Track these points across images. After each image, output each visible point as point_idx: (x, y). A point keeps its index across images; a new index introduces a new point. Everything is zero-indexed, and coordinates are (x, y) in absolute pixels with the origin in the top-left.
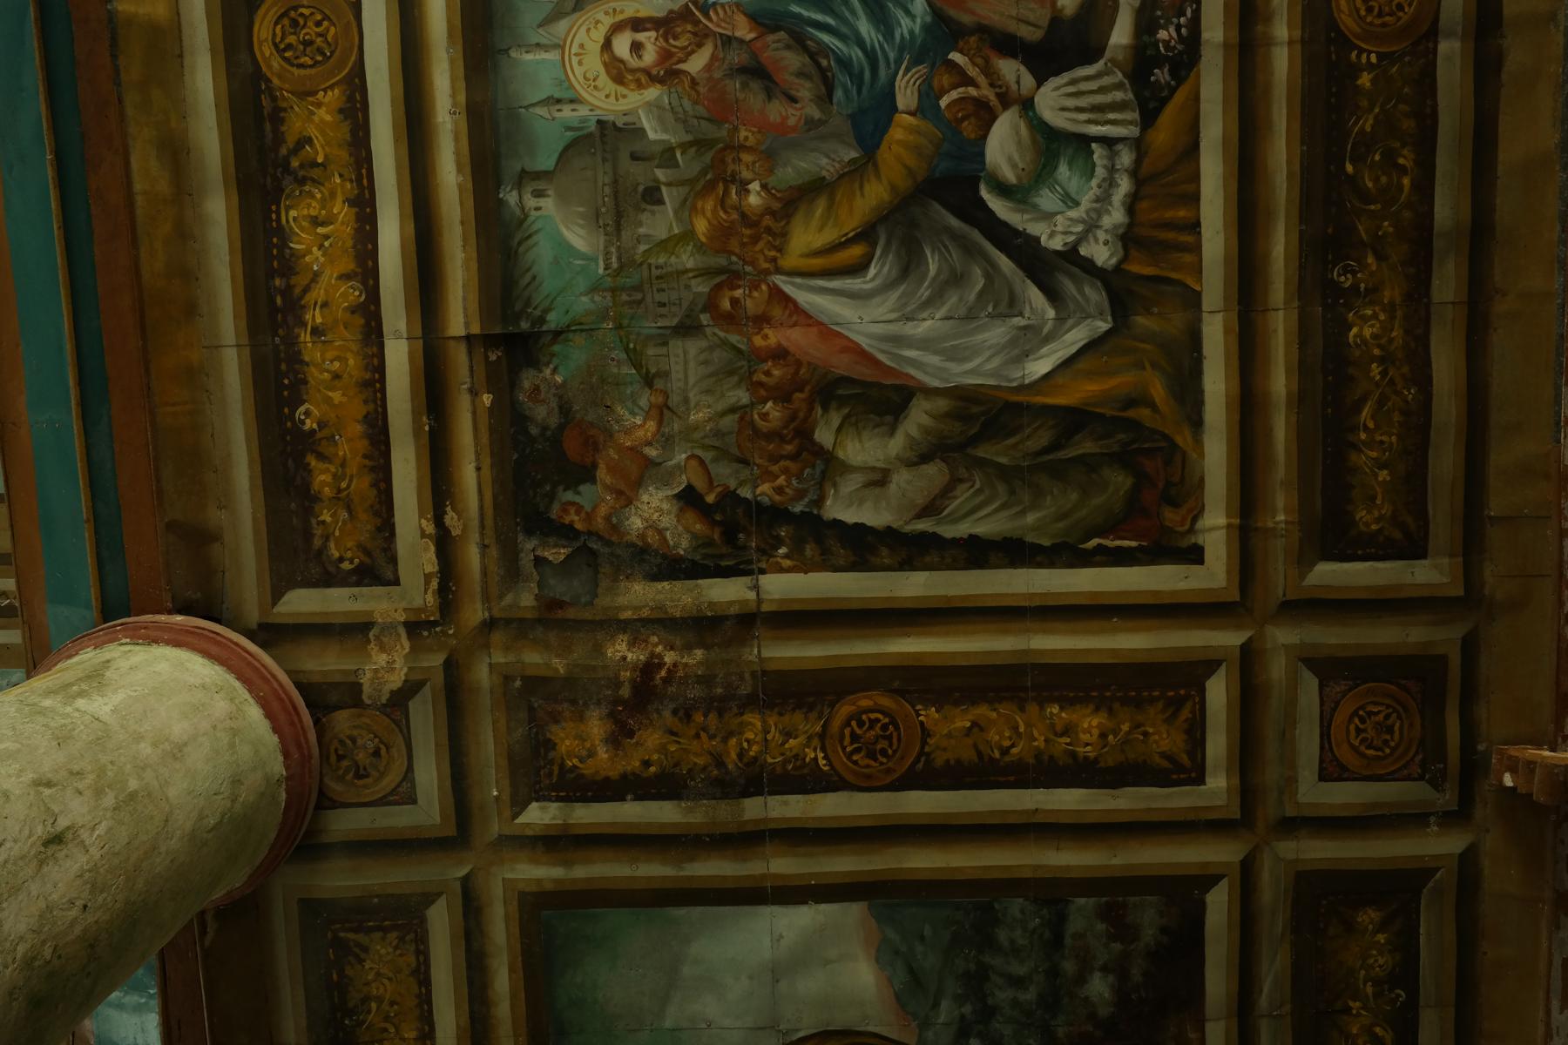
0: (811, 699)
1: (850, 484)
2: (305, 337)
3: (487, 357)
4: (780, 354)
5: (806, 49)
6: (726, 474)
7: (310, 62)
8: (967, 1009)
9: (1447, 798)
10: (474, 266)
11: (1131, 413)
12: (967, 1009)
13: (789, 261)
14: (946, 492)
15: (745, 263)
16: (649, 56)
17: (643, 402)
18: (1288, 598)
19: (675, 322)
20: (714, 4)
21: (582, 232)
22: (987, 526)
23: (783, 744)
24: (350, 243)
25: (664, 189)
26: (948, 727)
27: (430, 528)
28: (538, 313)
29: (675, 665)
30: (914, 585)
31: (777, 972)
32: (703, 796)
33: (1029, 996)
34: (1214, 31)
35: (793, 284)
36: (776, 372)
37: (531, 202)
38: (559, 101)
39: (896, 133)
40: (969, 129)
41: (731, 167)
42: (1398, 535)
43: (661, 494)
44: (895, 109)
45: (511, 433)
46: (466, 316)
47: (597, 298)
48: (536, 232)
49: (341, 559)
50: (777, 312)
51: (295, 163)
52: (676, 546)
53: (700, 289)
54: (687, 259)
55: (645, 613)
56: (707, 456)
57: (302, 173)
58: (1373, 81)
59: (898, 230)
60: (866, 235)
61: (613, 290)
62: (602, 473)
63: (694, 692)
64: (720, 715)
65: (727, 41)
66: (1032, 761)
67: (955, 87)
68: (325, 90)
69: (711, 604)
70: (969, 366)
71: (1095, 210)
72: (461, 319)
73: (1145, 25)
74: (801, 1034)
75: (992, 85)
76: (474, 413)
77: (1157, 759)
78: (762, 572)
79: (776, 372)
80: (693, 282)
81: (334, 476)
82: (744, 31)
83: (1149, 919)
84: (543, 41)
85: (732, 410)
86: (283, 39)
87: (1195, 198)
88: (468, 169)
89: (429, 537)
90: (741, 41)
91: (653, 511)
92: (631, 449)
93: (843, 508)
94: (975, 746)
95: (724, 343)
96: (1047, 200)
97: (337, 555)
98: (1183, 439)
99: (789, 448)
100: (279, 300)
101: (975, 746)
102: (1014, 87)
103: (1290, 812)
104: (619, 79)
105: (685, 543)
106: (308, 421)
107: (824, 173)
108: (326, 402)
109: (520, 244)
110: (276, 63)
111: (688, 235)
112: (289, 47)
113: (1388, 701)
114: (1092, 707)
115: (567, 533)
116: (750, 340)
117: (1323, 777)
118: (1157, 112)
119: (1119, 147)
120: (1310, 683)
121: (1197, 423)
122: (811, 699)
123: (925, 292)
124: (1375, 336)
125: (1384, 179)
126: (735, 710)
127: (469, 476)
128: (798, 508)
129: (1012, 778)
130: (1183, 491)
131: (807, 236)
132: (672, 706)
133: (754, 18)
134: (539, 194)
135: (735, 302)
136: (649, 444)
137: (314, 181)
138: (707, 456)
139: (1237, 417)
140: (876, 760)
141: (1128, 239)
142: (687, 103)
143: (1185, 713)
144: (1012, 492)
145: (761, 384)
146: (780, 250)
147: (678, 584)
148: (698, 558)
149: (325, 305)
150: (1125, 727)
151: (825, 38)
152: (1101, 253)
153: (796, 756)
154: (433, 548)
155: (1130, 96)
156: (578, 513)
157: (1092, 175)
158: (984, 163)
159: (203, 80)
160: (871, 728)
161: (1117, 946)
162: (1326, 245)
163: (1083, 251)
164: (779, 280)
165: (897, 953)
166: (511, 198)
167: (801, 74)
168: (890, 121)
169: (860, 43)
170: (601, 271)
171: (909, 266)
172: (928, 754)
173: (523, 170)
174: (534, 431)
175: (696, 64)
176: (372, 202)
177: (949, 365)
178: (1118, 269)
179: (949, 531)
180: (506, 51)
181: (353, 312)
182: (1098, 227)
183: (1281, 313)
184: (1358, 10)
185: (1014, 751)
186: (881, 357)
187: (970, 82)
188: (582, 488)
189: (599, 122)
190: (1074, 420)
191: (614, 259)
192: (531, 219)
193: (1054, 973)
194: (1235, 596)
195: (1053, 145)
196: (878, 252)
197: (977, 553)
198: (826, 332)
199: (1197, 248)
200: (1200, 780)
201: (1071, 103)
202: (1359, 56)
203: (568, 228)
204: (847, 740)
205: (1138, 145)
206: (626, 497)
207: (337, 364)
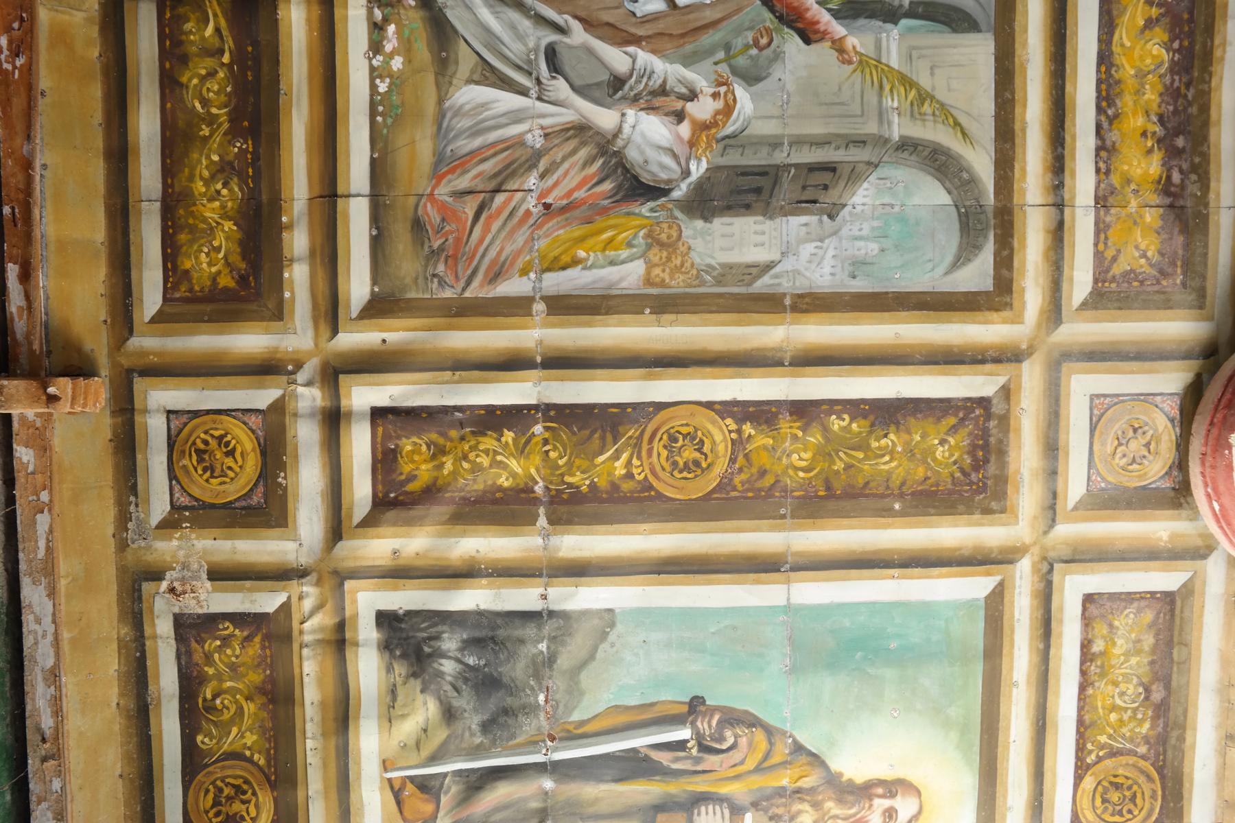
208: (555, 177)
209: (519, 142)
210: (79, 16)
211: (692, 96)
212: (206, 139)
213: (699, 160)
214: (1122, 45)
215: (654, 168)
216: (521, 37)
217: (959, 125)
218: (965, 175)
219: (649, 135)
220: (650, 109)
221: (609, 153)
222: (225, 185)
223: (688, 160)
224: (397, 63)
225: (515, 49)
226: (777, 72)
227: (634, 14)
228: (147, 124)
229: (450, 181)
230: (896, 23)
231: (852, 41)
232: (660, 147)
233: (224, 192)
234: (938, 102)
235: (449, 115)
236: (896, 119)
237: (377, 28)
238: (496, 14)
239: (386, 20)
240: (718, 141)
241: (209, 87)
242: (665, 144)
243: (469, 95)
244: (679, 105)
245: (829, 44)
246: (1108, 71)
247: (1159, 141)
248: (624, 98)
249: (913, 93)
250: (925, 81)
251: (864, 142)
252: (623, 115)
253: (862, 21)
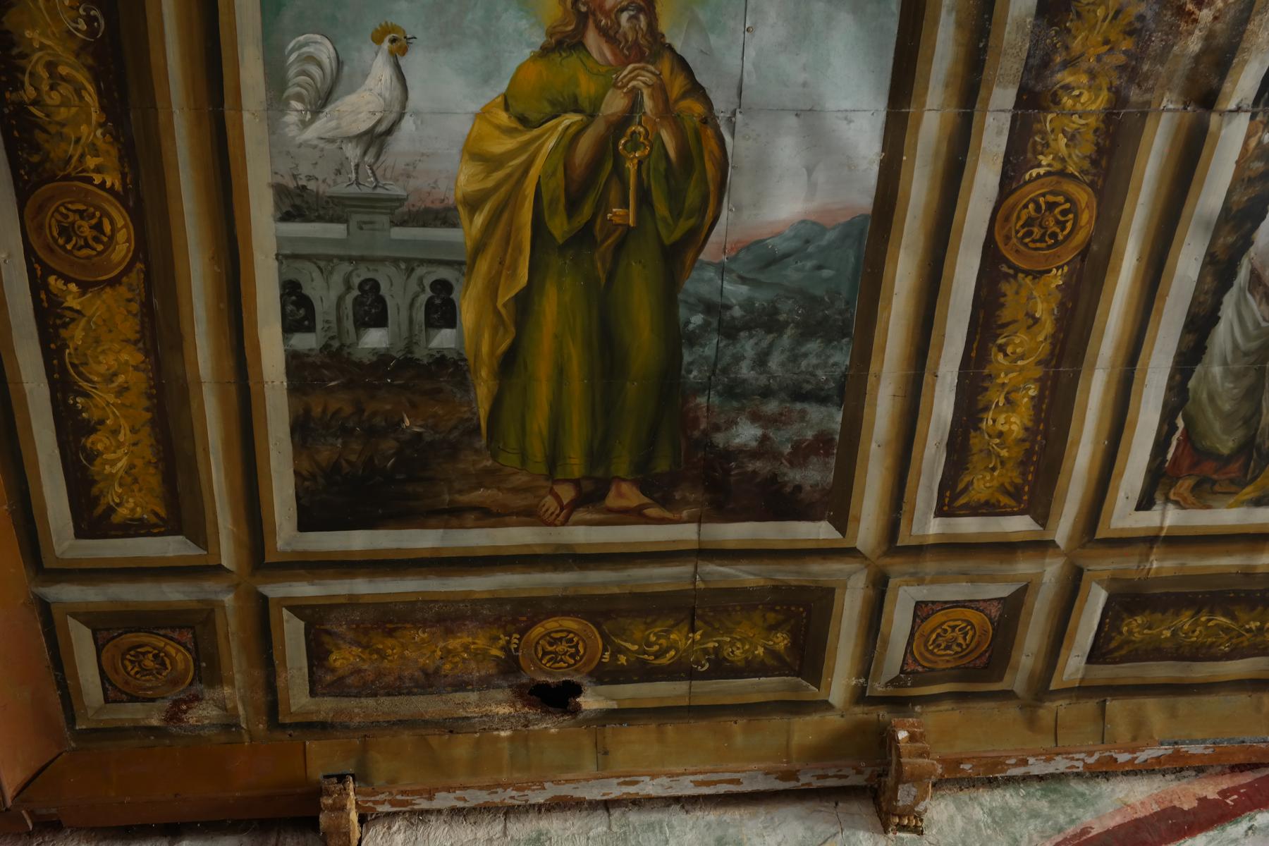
0: (1104, 163)
8: (737, 312)
9: (878, 688)
12: (737, 312)
18: (1086, 575)
22: (1223, 336)
23: (1064, 132)
26: (1040, 299)
29: (1196, 21)
31: (810, 115)
32: (1035, 44)
33: (745, 371)
42: (1113, 645)
63: (1156, 44)
64: (1118, 67)
66: (986, 371)
69: (1245, 62)
74: (728, 138)
77: (967, 479)
83: (814, 475)
94: (1014, 321)
98: (1249, 492)
101: (1014, 321)
103: (892, 582)
113: (973, 645)
114: (1030, 424)
117: (919, 604)
120: (1003, 591)
122: (1104, 163)
126: (1116, 82)
129: (973, 354)
130: (1203, 494)
132: (1149, 15)
139: (1252, 531)
140: (1023, 226)
143: (1005, 500)
144: (1246, 354)
150: (1004, 453)
153: (1047, 145)
160: (1058, 222)
161: (787, 449)
165: (807, 242)
172: (1015, 277)
179: (1229, 300)
185: (1000, 357)
193: (766, 393)
197: (1200, 323)
200: (940, 513)
204: (1051, 198)
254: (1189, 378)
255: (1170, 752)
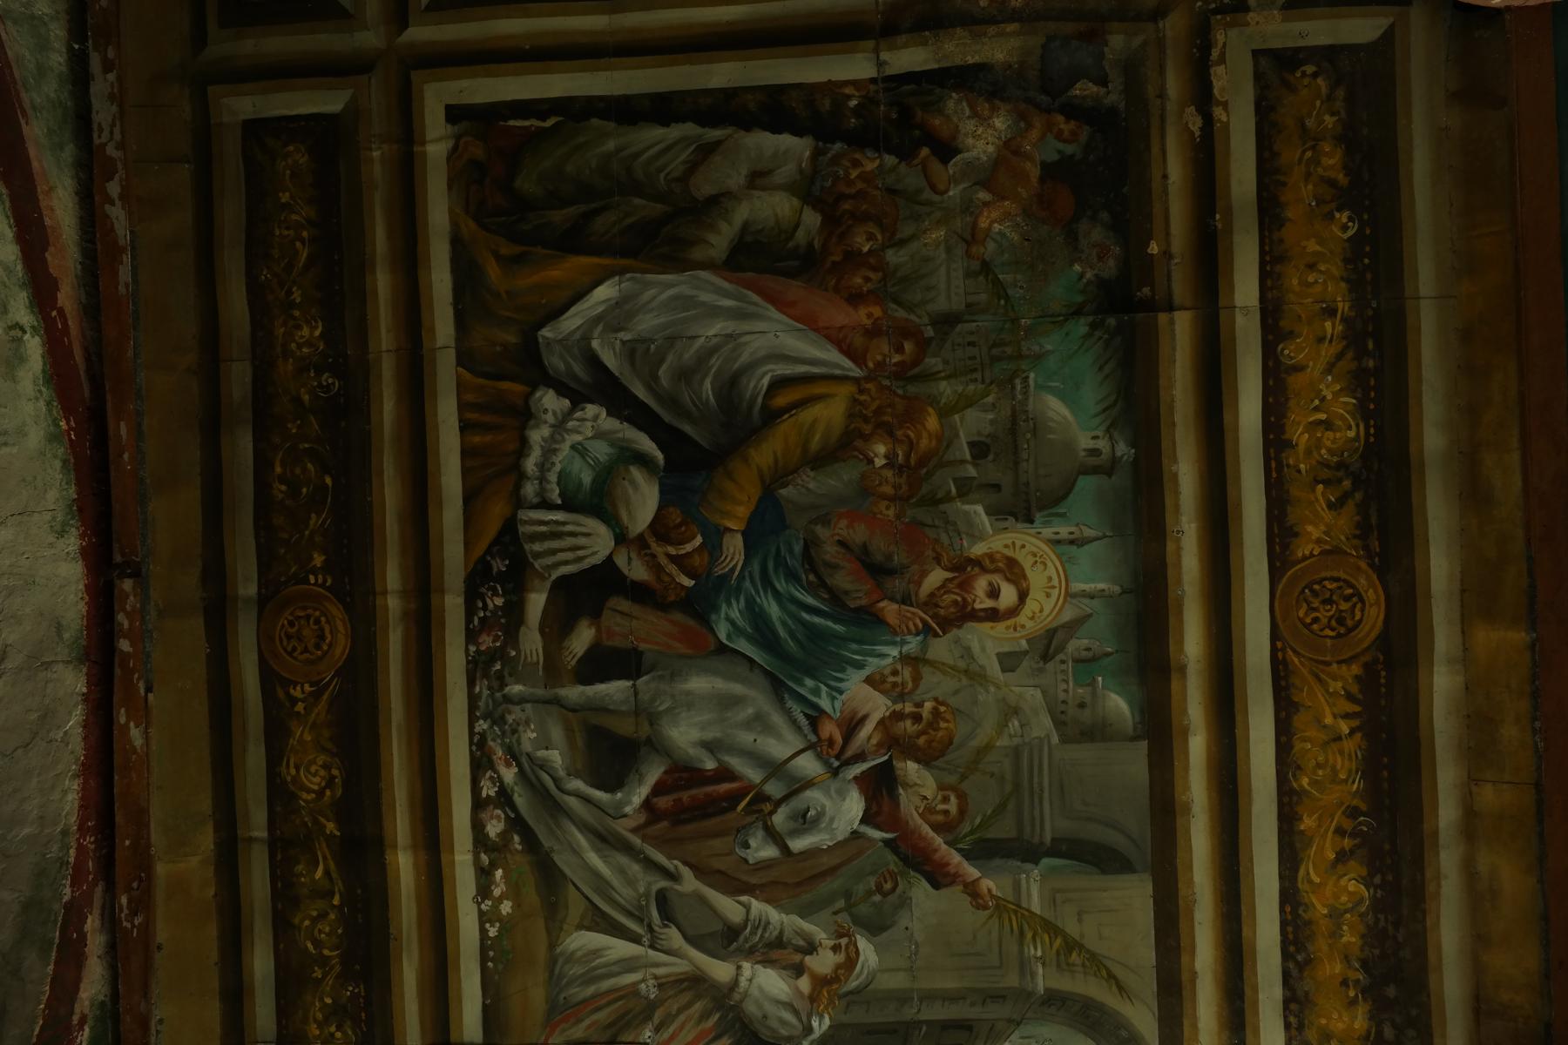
1: (786, 172)
2: (1343, 307)
3: (1152, 290)
4: (855, 299)
5: (830, 590)
6: (910, 178)
7: (1326, 583)
10: (1162, 382)
11: (518, 249)
13: (846, 390)
14: (693, 167)
15: (888, 388)
16: (981, 585)
17: (991, 246)
19: (959, 328)
20: (917, 634)
21: (1050, 414)
22: (653, 136)
24: (1292, 403)
25: (968, 457)
27: (1218, 112)
28: (1097, 334)
30: (722, 74)
34: (453, 604)
35: (843, 368)
36: (859, 280)
37: (1103, 444)
38: (1072, 542)
39: (743, 511)
40: (675, 516)
41: (903, 480)
43: (974, 153)
44: (744, 533)
45: (1130, 216)
46: (1173, 331)
47: (1036, 348)
48: (1096, 415)
49: (1315, 75)
50: (858, 341)
51: (1347, 484)
52: (959, 101)
53: (933, 361)
54: (946, 389)
55: (992, 30)
56: (928, 194)
57: (1341, 474)
58: (311, 559)
59: (741, 420)
60: (772, 416)
61: (1020, 357)
62: (1035, 173)
65: (906, 600)
67: (688, 555)
68: (1312, 555)
69: (925, 43)
70: (671, 292)
71: (556, 442)
72: (1178, 328)
73: (515, 612)
75: (654, 556)
76: (1168, 234)
78: (873, 81)
79: (859, 280)
80: (940, 367)
81: (1318, 163)
82: (889, 609)
84: (1087, 601)
85: (902, 243)
86: (1354, 606)
87: (466, 453)
88: (1166, 477)
89: (1219, 103)
90: (892, 599)
91: (982, 135)
92: (1004, 198)
93: (792, 148)
95: (910, 309)
96: (602, 451)
97: (1320, 81)
98: (469, 226)
99: (847, 206)
100: (1371, 345)
102: (633, 555)
104: (1012, 563)
105: (951, 104)
106: (1344, 220)
107: (812, 474)
108: (1321, 240)
109: (1116, 402)
110: (1362, 582)
111: (944, 413)
112: (1347, 599)
115: (1072, 111)
116: (885, 312)
118: (501, 534)
119: (536, 500)
121: (456, 242)
123: (715, 362)
124: (299, 327)
125: (298, 471)
127: (1174, 169)
128: (838, 146)
130: (468, 177)
131: (829, 414)
133: (879, 621)
134: (1094, 452)
135: (900, 349)
136: (986, 204)
137: (1328, 466)
138: (928, 194)
141: (525, 415)
142: (944, 539)
145: (875, 269)
146: (855, 400)
147: (958, 61)
148: (938, 90)
149: (1321, 340)
151: (810, 600)
152: (550, 402)
154: (1216, 91)
155: (527, 547)
156: (1061, 132)
157: (560, 473)
158: (661, 485)
159: (1440, 567)
162: (347, 412)
163: (567, 403)
164: (856, 372)
166: (1122, 449)
167: (835, 567)
168: (750, 522)
169: (777, 595)
170: (1032, 375)
171: (730, 385)
173: (1110, 475)
174: (1105, 216)
175: (936, 577)
176: (1267, 444)
177: (694, 292)
178: (534, 387)
179: (689, 129)
180: (1124, 592)
181: (1291, 332)
182: (552, 426)
183: (384, 348)
184: (328, 622)
186: (755, 298)
187: (674, 559)
188: (1056, 157)
189: (1032, 522)
190: (571, 241)
191: (1019, 387)
192: (1103, 428)
194: (416, 76)
195: (598, 501)
196: (760, 400)
197: (662, 108)
198: (809, 322)
199: (462, 407)
201: (582, 541)
202: (325, 581)
203: (1065, 418)
205: (518, 502)
206: (1010, 148)
207: (1311, 279)
208: (671, 1030)
209: (633, 991)
210: (194, 861)
211: (811, 948)
212: (319, 982)
213: (821, 1017)
214: (1310, 882)
215: (774, 1024)
216: (631, 883)
217: (1115, 978)
218: (1124, 1033)
219: (767, 984)
220: (767, 962)
221: (725, 1004)
222: (339, 1028)
223: (809, 1016)
224: (506, 908)
225: (625, 893)
226: (904, 921)
227: (746, 861)
228: (261, 963)
229: (564, 1031)
230: (1037, 864)
231: (987, 884)
232: (778, 1002)
233: (338, 1035)
234: (1088, 951)
235: (560, 961)
236: (1040, 971)
237: (484, 875)
238: (604, 858)
239: (493, 865)
240: (840, 997)
241: (321, 930)
242: (783, 997)
243: (582, 940)
244: (797, 958)
245: (961, 887)
246: (1294, 912)
247: (1363, 992)
248: (739, 950)
249: (1059, 941)
250: (1072, 928)
251: (1004, 997)
252: (739, 968)
253: (997, 862)
254: (601, 118)
255: (122, 242)
